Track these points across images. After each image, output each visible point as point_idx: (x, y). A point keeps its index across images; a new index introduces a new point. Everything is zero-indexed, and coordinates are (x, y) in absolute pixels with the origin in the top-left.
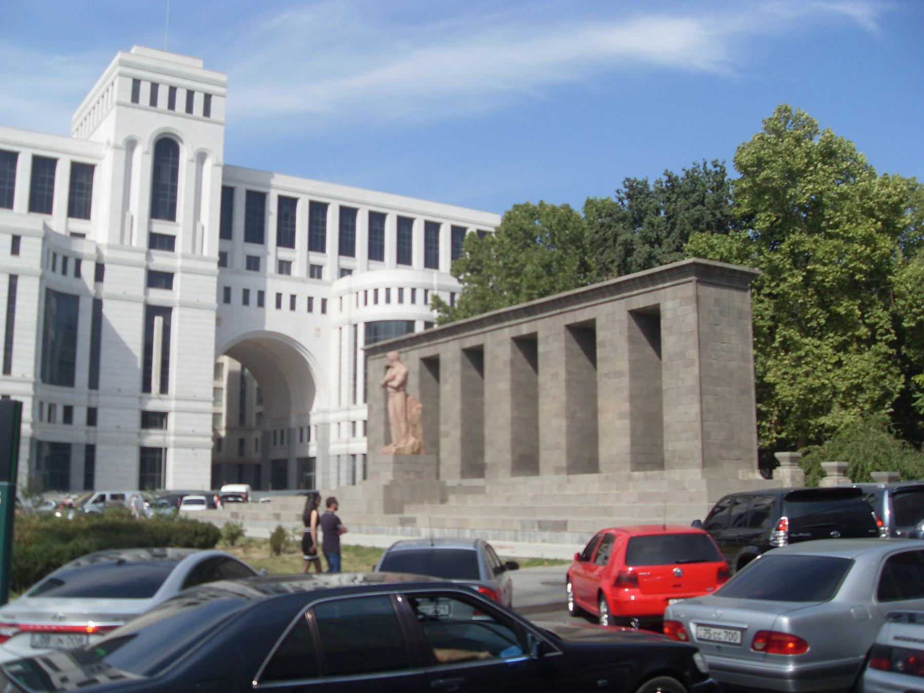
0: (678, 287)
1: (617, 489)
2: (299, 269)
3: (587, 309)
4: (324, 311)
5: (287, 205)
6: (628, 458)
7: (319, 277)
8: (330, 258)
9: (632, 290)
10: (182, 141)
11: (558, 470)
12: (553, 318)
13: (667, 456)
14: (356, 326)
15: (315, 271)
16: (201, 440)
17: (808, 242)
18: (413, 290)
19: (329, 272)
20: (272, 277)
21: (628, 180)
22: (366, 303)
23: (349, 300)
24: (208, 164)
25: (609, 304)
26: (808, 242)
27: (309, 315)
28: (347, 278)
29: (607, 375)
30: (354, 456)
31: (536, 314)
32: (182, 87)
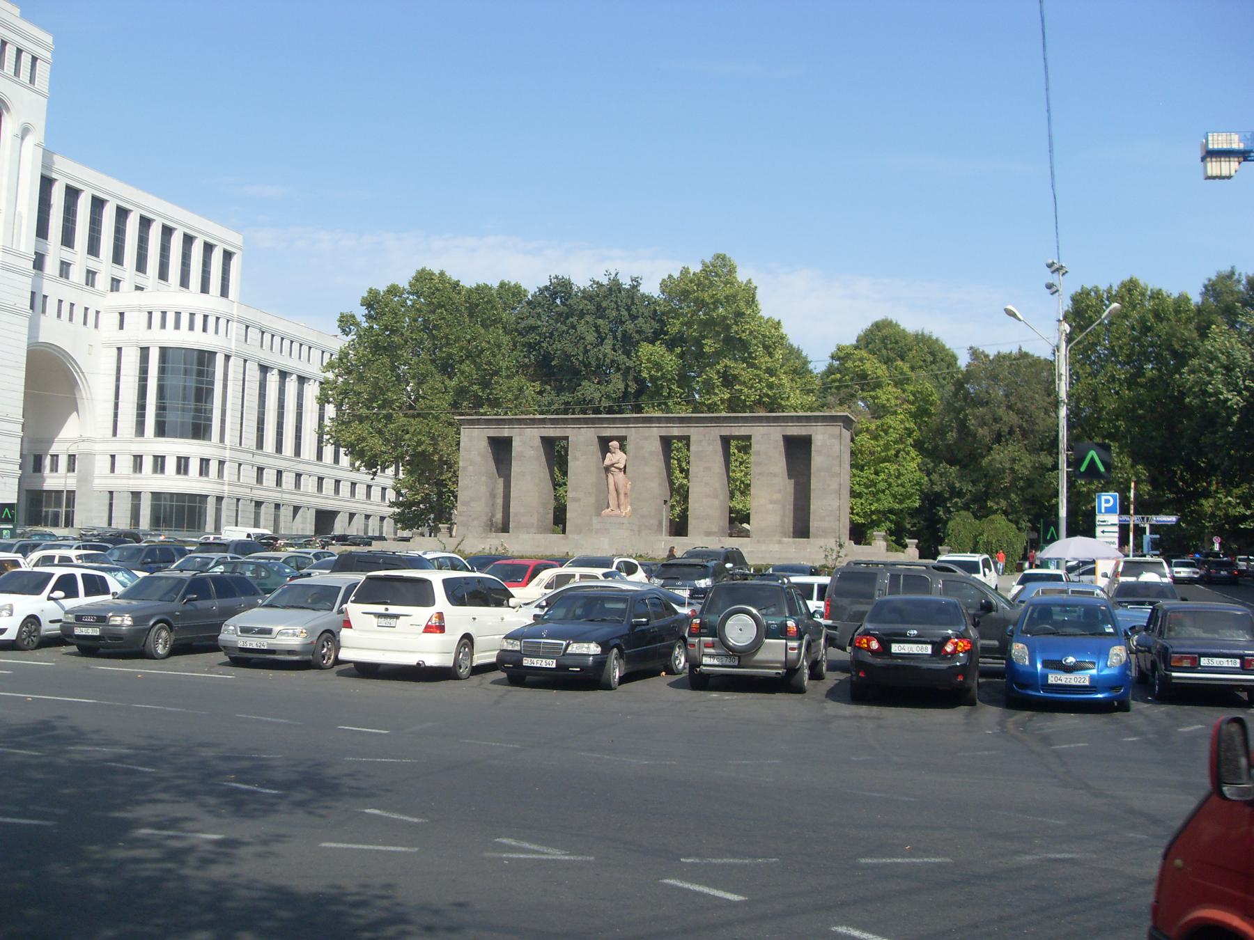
2: (77, 274)
4: (96, 326)
5: (72, 194)
7: (93, 285)
8: (104, 264)
10: (8, 109)
11: (708, 534)
14: (145, 352)
15: (91, 275)
16: (10, 466)
17: (738, 368)
18: (218, 319)
19: (102, 282)
20: (51, 279)
21: (557, 277)
22: (163, 326)
23: (136, 321)
24: (30, 140)
26: (738, 368)
27: (84, 328)
28: (139, 292)
30: (136, 495)
32: (13, 44)
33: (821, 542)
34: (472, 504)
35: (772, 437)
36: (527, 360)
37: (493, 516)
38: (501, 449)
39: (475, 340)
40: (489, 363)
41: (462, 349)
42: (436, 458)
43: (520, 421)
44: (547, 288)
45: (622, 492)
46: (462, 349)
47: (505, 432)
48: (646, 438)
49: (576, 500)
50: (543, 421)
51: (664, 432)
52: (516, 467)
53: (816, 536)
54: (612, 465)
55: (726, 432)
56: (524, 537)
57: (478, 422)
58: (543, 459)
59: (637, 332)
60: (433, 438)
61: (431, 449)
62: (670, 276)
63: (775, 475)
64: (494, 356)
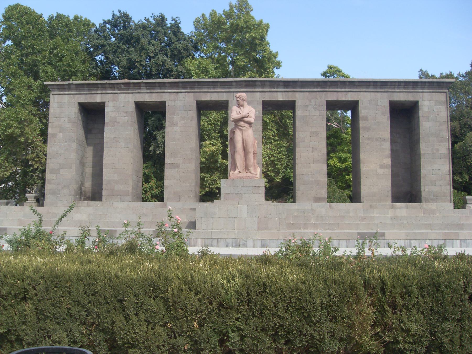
0: (434, 94)
1: (424, 214)
3: (350, 93)
6: (390, 194)
9: (394, 88)
11: (317, 200)
13: (423, 194)
25: (372, 93)
29: (369, 139)
31: (294, 88)
33: (432, 206)
34: (62, 171)
35: (379, 104)
36: (95, 71)
37: (82, 184)
38: (92, 115)
39: (56, 49)
40: (69, 65)
41: (45, 57)
42: (22, 139)
43: (113, 86)
44: (109, 22)
45: (251, 150)
46: (45, 57)
47: (98, 99)
50: (138, 86)
51: (268, 97)
52: (109, 133)
53: (427, 201)
54: (241, 119)
55: (333, 97)
56: (119, 205)
57: (69, 87)
58: (136, 126)
59: (184, 49)
60: (20, 123)
61: (18, 132)
62: (203, 15)
63: (384, 140)
64: (73, 61)
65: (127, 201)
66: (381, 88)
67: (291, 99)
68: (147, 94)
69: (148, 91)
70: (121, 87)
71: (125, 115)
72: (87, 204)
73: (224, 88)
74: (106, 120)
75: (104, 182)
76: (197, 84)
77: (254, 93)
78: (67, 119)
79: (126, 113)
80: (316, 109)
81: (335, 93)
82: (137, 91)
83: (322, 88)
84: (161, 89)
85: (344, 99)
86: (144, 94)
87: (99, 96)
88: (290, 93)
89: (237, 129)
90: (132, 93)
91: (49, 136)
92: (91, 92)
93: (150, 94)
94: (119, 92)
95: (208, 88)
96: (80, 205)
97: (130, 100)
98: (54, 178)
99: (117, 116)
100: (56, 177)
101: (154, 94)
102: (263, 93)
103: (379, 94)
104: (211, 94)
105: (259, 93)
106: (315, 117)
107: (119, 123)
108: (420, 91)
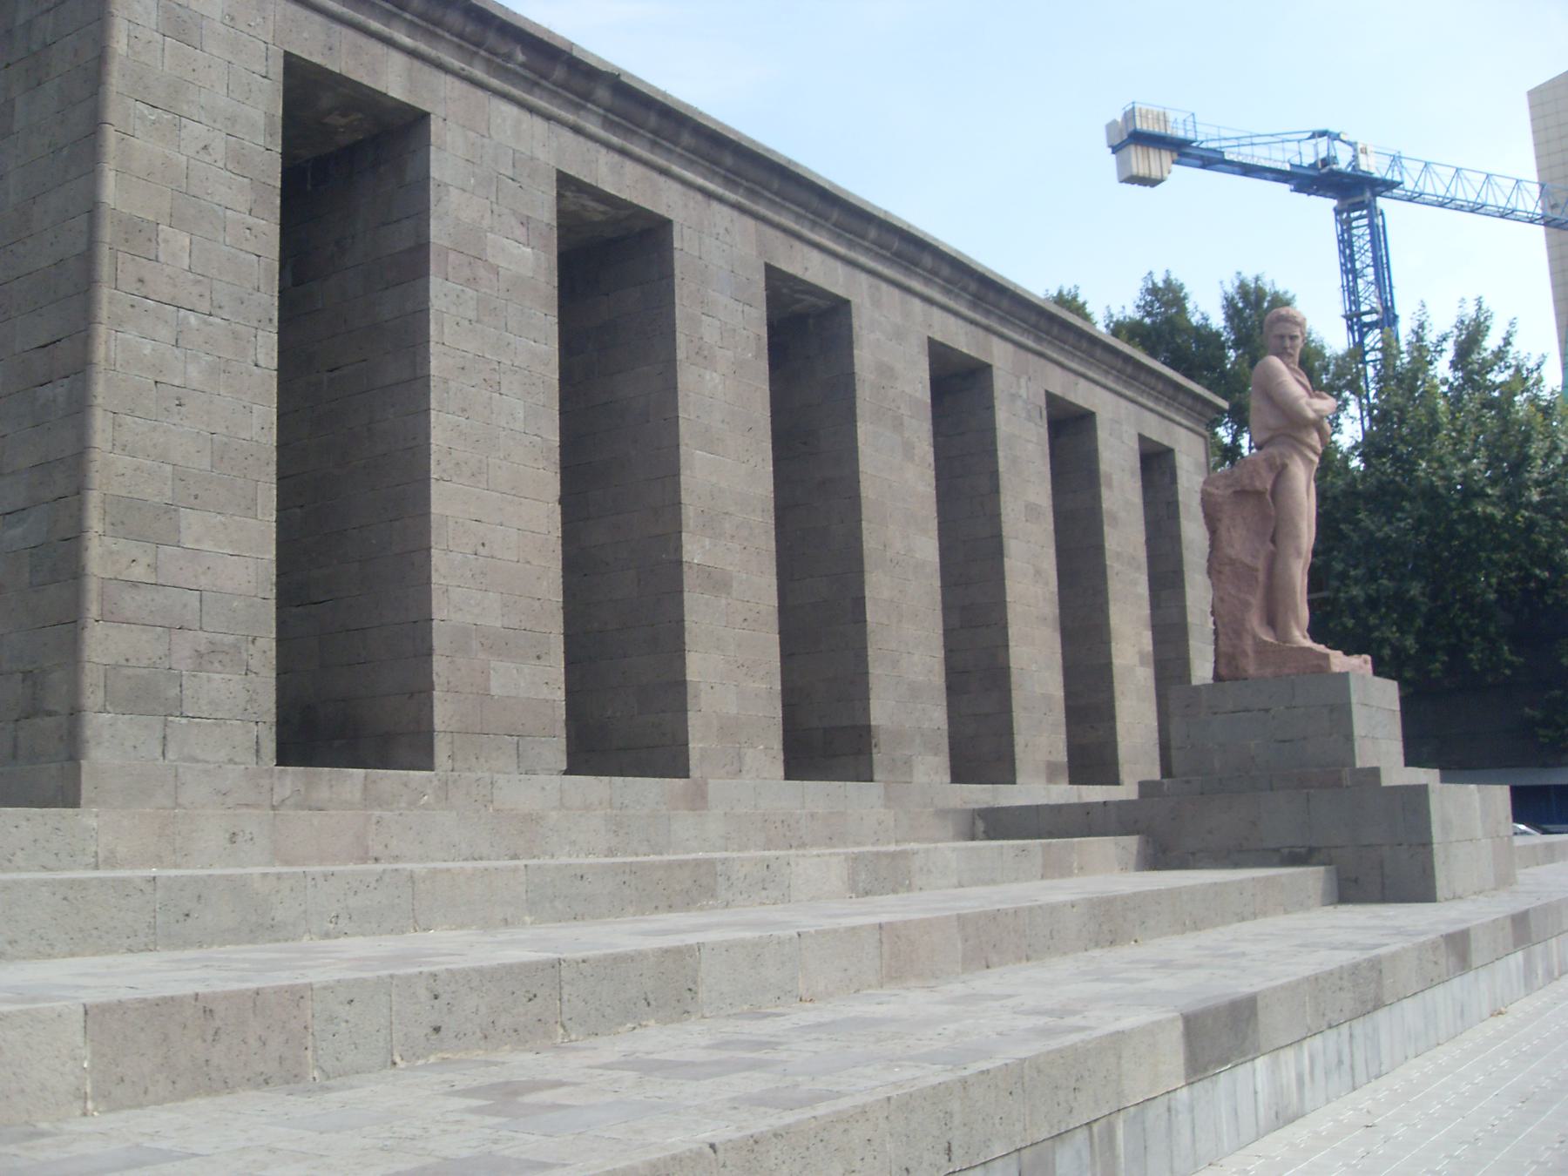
12: (1022, 353)
29: (1118, 555)
31: (987, 313)
34: (193, 524)
47: (392, 77)
48: (899, 335)
49: (718, 583)
65: (550, 772)
66: (1128, 385)
67: (984, 358)
68: (603, 151)
69: (615, 140)
70: (509, 57)
71: (520, 232)
72: (365, 789)
73: (838, 238)
74: (439, 233)
75: (439, 641)
76: (776, 185)
77: (908, 298)
78: (219, 145)
79: (525, 222)
80: (1029, 418)
81: (1058, 370)
82: (570, 117)
83: (1038, 339)
84: (654, 145)
85: (1072, 397)
86: (590, 144)
87: (398, 59)
88: (980, 333)
89: (1297, 458)
90: (548, 117)
91: (107, 233)
92: (359, 17)
93: (616, 158)
94: (495, 83)
95: (798, 217)
96: (323, 793)
97: (541, 154)
98: (139, 572)
99: (486, 223)
100: (154, 567)
101: (630, 167)
102: (927, 307)
103: (1123, 403)
104: (806, 249)
105: (917, 304)
106: (1030, 447)
107: (495, 270)
108: (1178, 418)
